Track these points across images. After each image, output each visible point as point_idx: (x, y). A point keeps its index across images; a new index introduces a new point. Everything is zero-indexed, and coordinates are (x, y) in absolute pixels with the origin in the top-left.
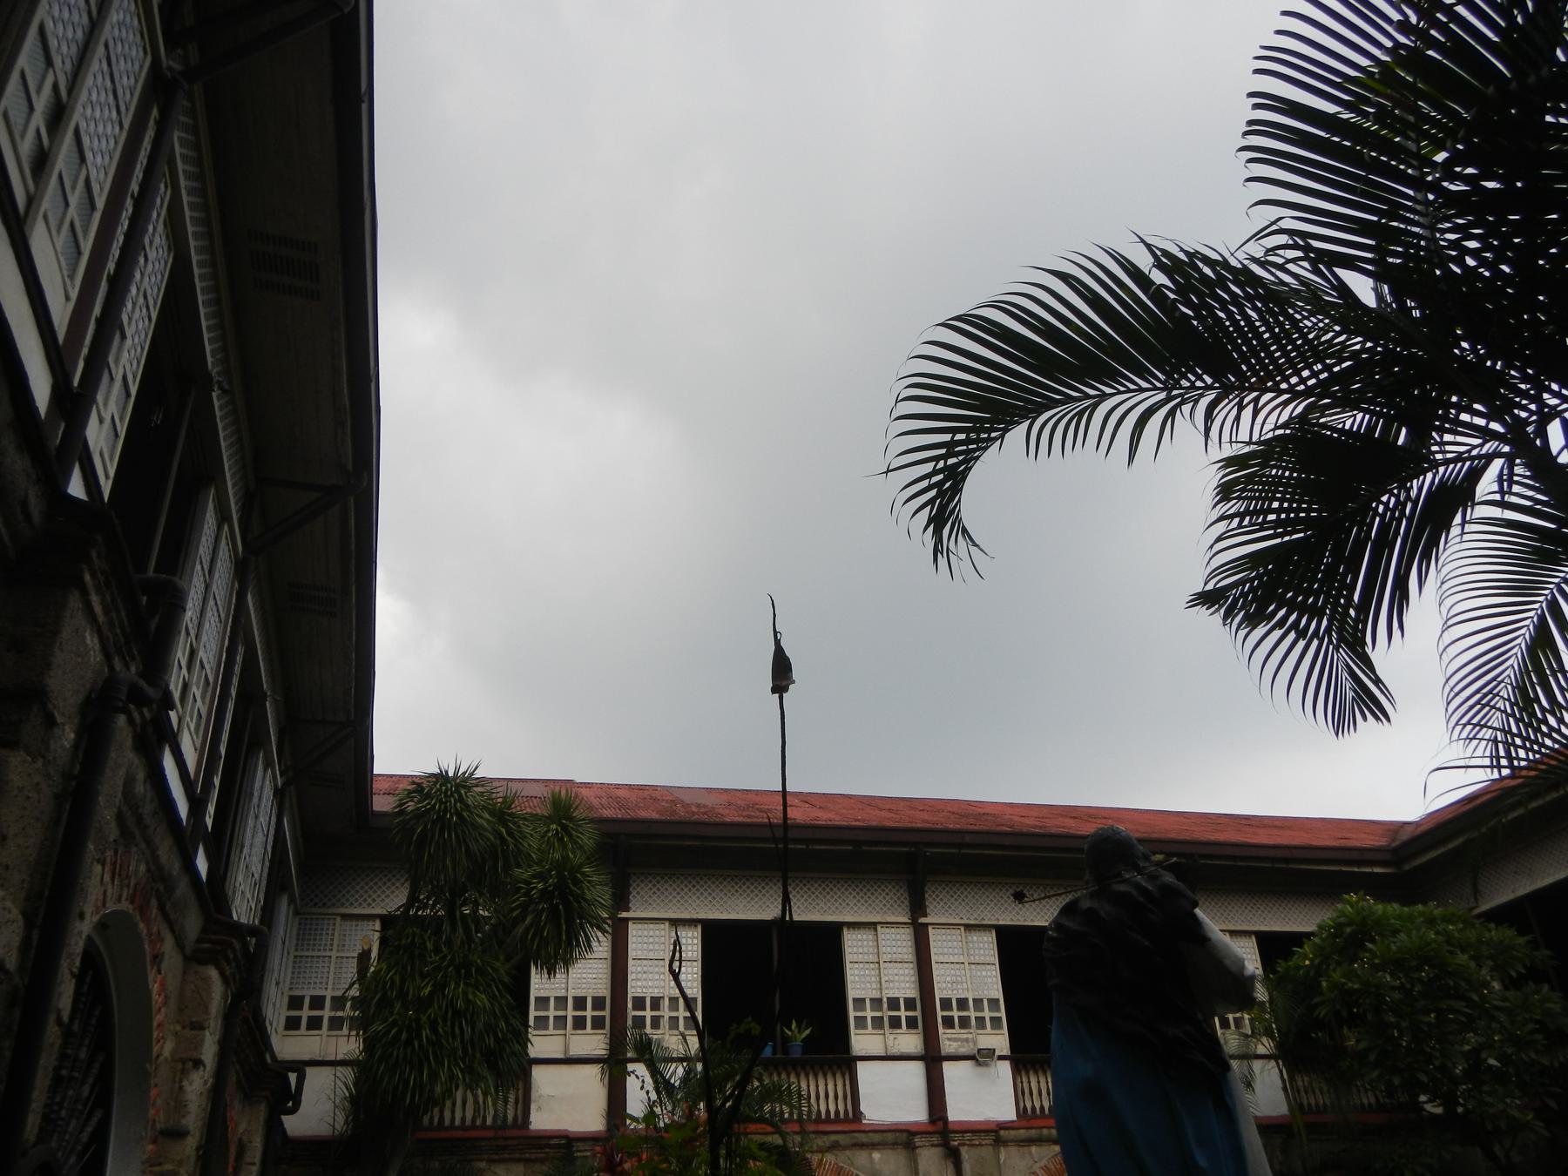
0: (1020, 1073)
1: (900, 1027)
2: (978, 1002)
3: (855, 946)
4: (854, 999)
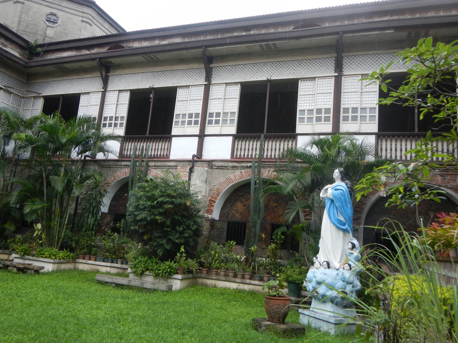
3: (180, 95)
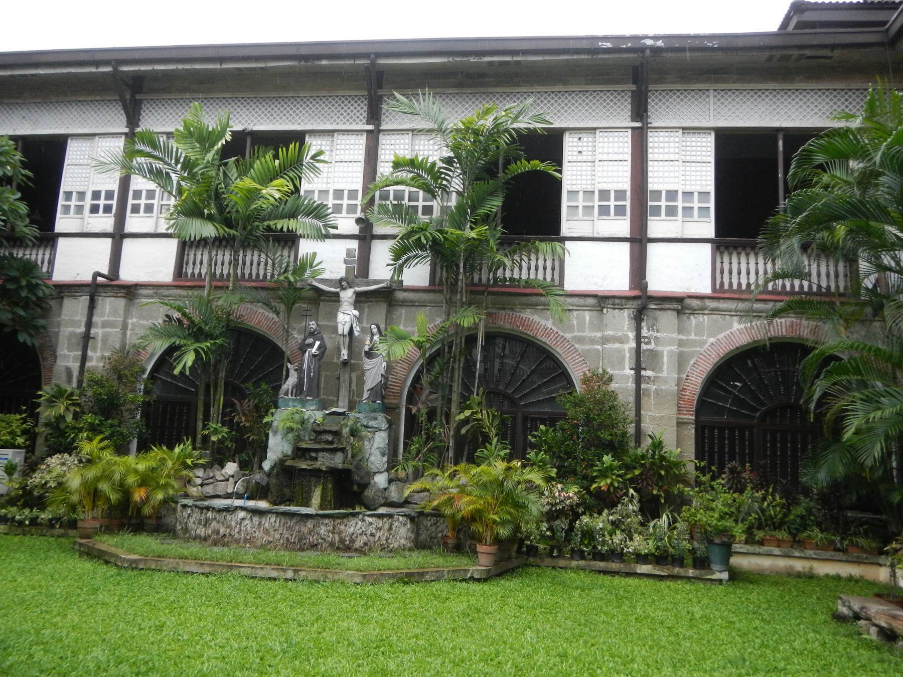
0: (722, 253)
1: (609, 214)
2: (688, 195)
4: (569, 192)
